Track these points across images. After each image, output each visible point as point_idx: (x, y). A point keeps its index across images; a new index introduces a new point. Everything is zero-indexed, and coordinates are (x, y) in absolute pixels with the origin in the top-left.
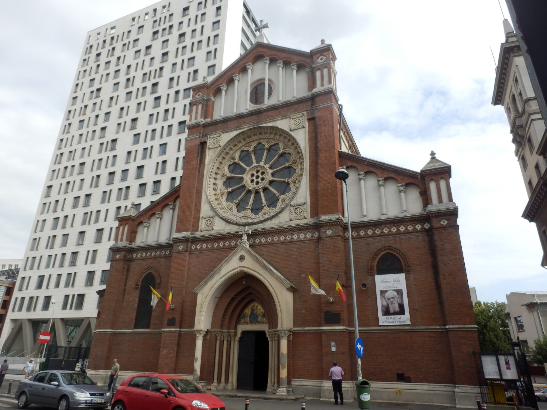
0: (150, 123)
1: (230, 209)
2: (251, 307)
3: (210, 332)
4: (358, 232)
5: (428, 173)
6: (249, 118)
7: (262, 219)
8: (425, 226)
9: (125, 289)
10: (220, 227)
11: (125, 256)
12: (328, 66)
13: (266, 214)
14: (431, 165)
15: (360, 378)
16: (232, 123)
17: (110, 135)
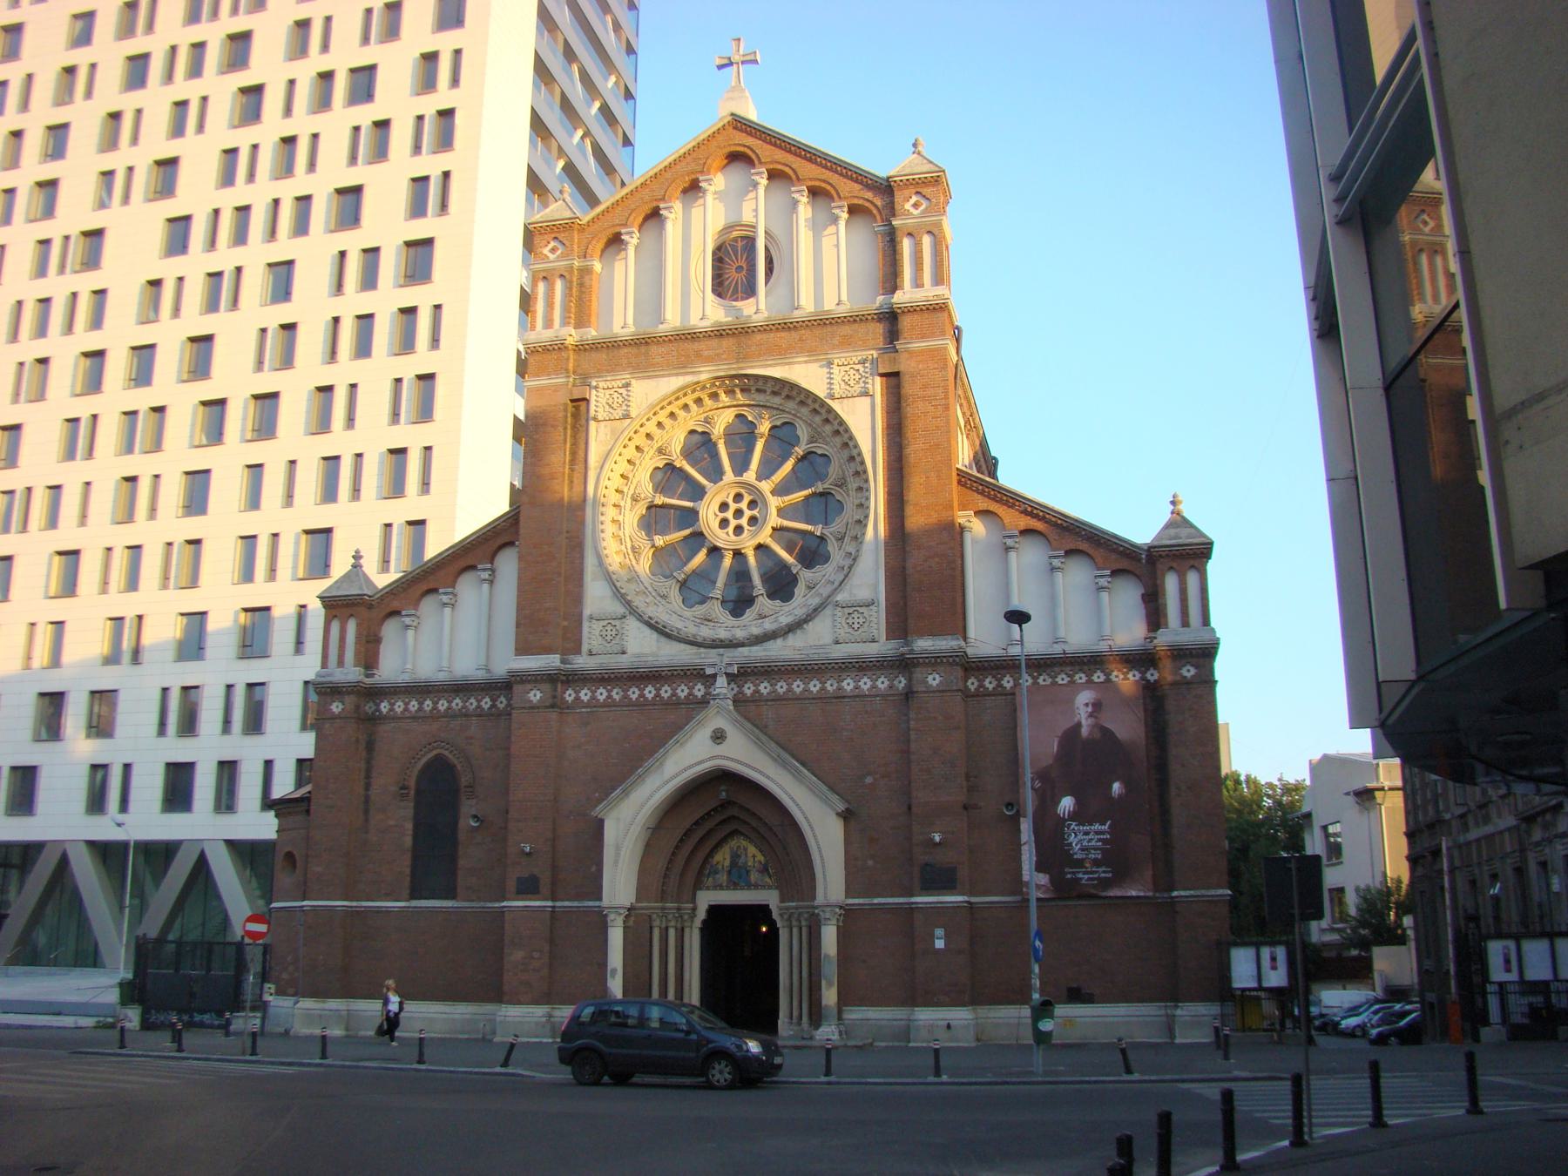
0: (227, 178)
1: (664, 597)
2: (731, 849)
3: (635, 909)
4: (999, 680)
5: (1163, 554)
6: (714, 343)
7: (756, 631)
8: (1148, 676)
9: (367, 800)
10: (642, 647)
11: (357, 707)
12: (935, 231)
13: (765, 617)
14: (1172, 532)
15: (1036, 996)
16: (661, 350)
17: (75, 214)
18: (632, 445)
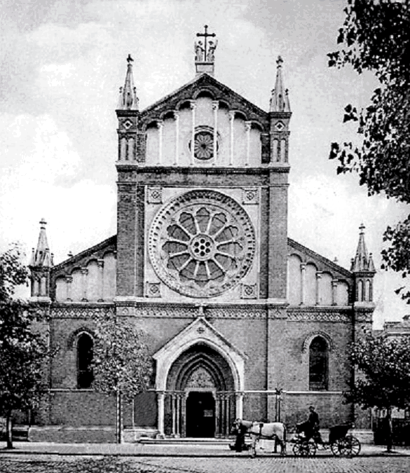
18: (160, 217)
